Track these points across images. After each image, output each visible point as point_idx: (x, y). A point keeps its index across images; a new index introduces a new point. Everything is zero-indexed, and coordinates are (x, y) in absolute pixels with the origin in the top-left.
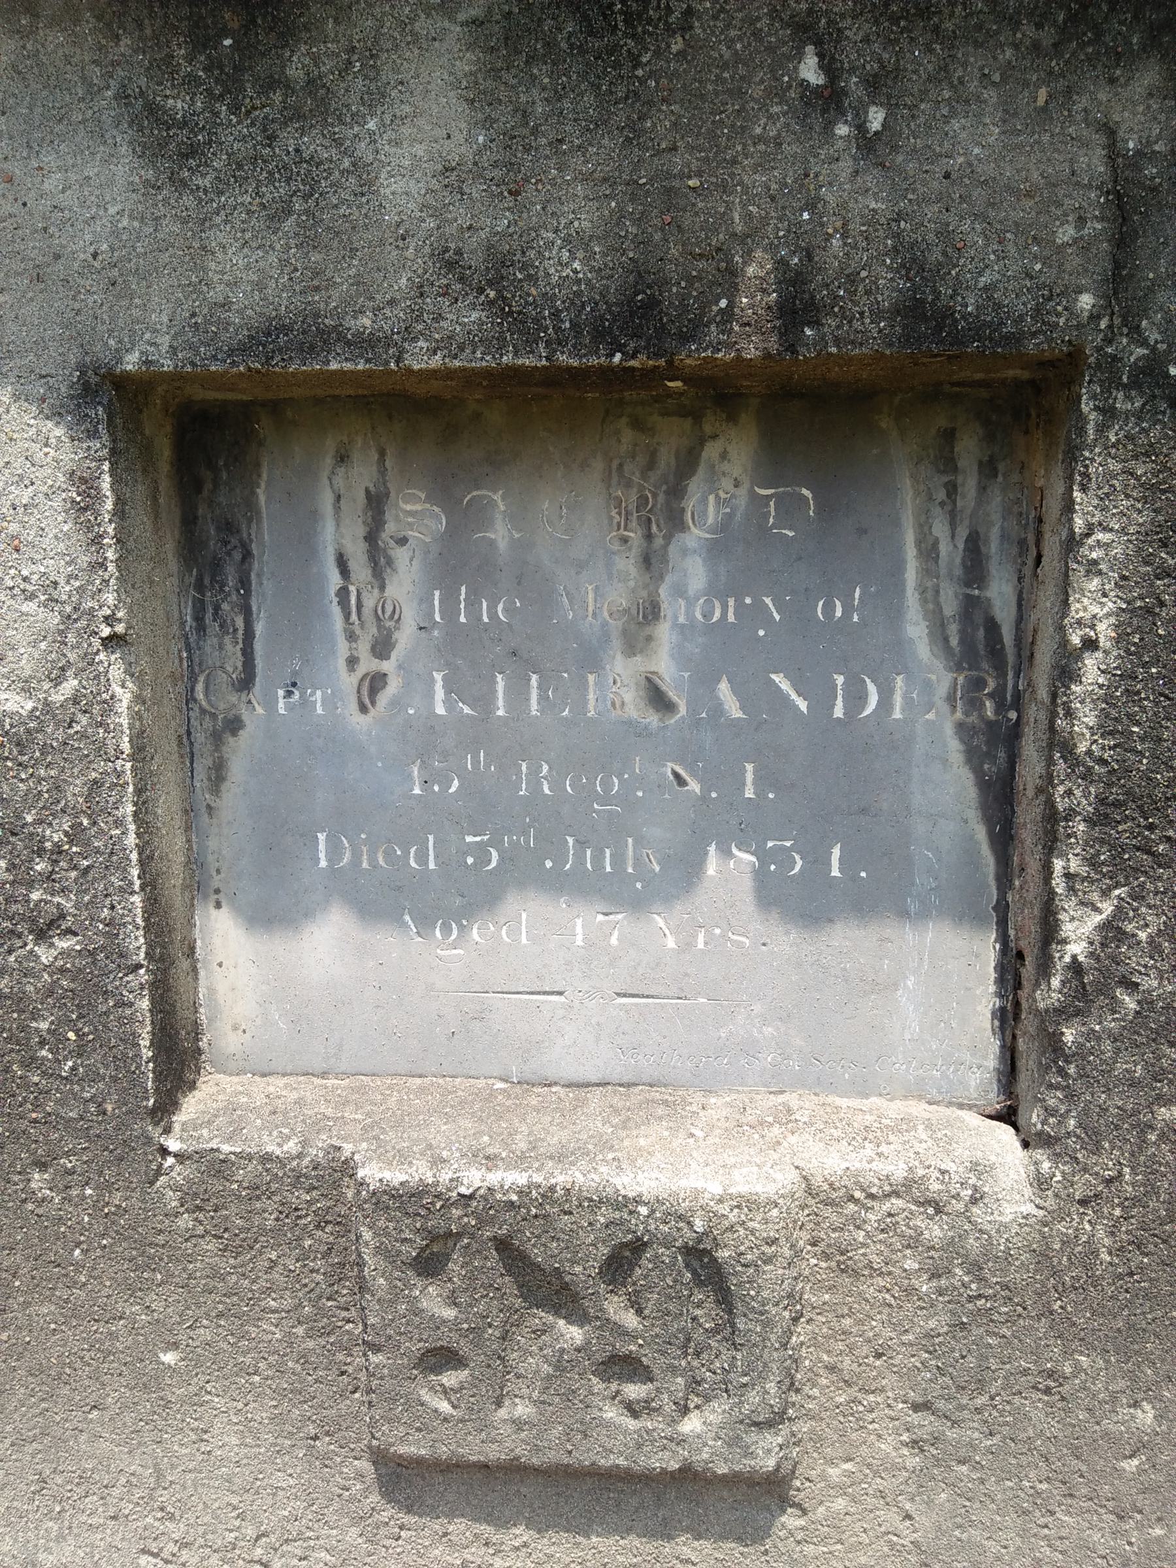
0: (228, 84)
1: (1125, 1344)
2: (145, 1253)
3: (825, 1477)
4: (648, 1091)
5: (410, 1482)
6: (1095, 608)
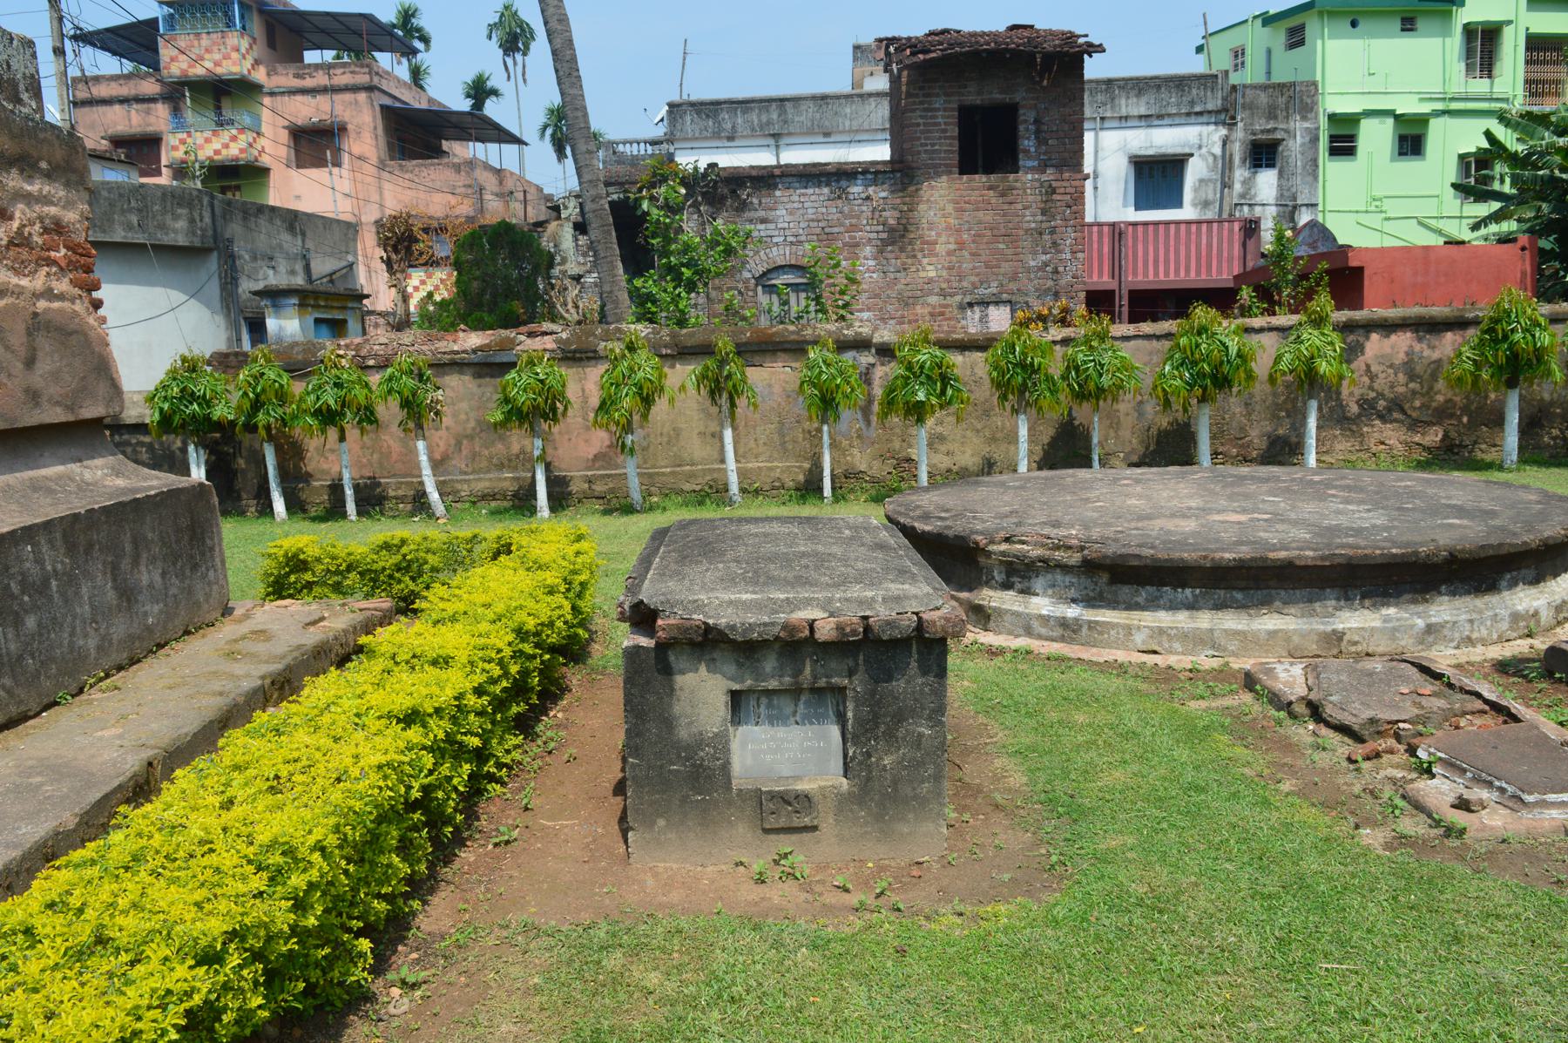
0: (747, 658)
1: (860, 804)
2: (730, 803)
3: (823, 826)
4: (797, 778)
5: (767, 831)
6: (850, 714)
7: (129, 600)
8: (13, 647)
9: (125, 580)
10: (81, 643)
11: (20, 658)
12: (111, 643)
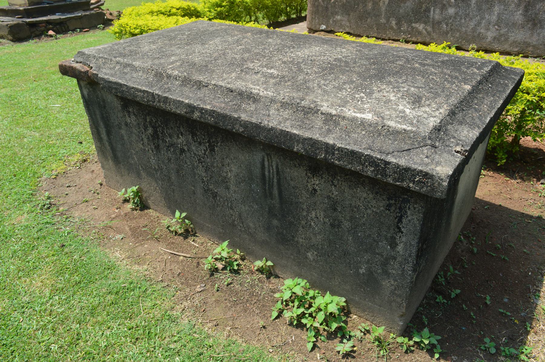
7: (535, 25)
8: (437, 17)
9: (536, 14)
10: (482, 31)
11: (439, 23)
12: (507, 40)
